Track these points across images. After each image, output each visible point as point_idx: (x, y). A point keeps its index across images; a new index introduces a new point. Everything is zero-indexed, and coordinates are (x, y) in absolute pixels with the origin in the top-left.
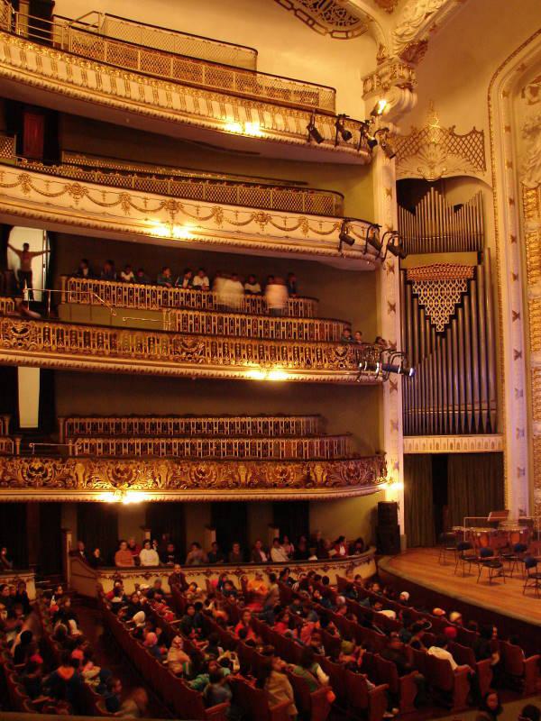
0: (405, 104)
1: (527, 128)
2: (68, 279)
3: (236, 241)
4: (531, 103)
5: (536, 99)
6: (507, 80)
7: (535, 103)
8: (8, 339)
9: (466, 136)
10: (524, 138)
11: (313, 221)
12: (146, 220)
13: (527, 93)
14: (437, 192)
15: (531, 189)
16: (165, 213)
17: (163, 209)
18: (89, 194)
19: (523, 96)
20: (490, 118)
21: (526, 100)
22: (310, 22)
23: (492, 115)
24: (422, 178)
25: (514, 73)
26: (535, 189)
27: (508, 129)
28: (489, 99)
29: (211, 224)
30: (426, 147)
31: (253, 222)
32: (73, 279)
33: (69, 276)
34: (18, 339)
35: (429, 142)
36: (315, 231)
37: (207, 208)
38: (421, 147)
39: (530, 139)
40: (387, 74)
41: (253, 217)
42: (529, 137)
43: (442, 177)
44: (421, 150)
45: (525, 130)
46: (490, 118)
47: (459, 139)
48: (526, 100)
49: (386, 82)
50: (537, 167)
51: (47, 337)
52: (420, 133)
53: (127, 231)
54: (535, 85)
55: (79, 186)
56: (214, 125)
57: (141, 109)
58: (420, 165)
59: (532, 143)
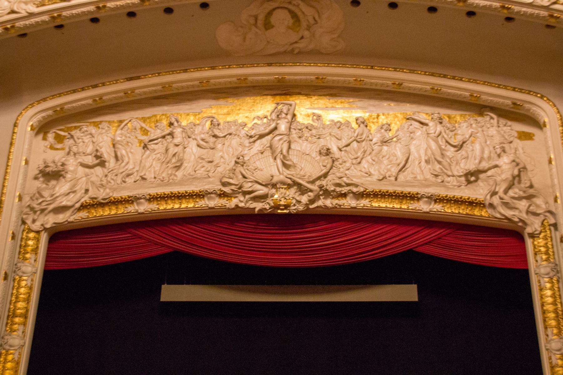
1: (48, 170)
4: (52, 148)
5: (59, 146)
6: (44, 114)
7: (57, 149)
10: (36, 178)
13: (51, 136)
15: (33, 231)
19: (44, 139)
20: (11, 144)
21: (47, 143)
23: (16, 142)
25: (50, 112)
26: (38, 232)
27: (27, 162)
28: (15, 125)
39: (43, 182)
42: (41, 179)
45: (41, 171)
46: (11, 144)
48: (47, 143)
50: (46, 212)
54: (62, 133)
59: (44, 186)
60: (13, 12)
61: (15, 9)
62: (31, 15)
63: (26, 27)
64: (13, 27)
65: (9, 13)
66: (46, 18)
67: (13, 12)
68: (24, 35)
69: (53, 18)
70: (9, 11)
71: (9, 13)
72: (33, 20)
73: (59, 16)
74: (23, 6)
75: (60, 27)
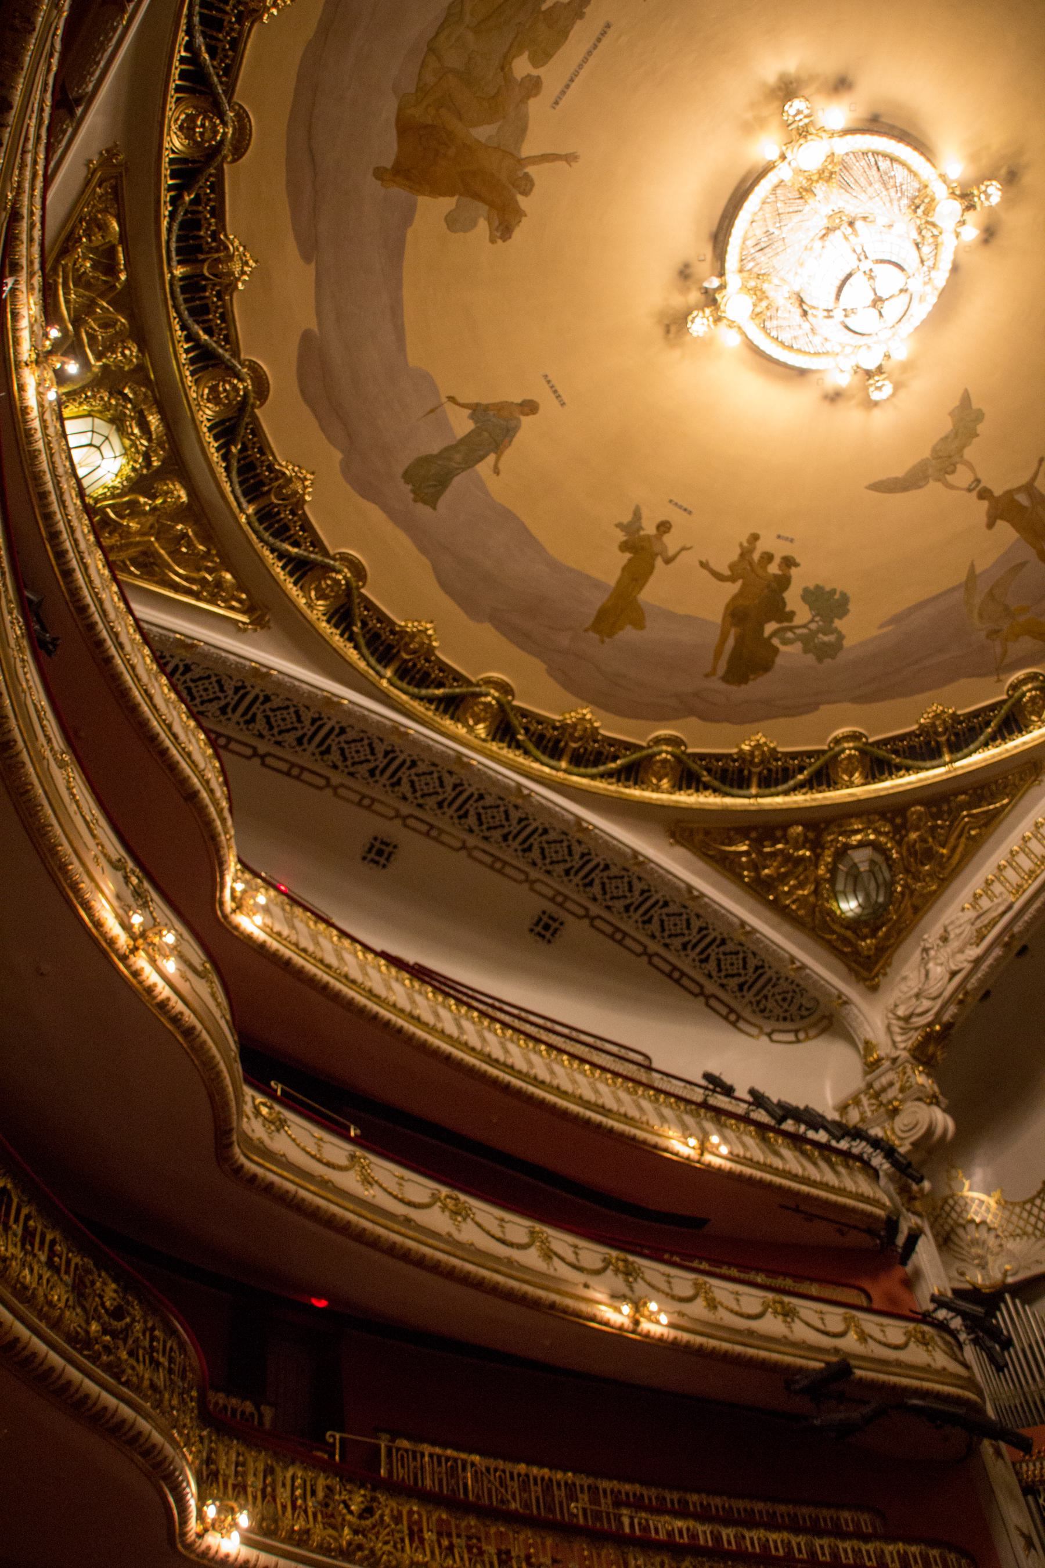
0: (939, 1131)
2: (393, 1441)
3: (751, 1351)
8: (334, 1528)
9: (1032, 1201)
11: (870, 1323)
12: (586, 1286)
14: (1017, 1301)
16: (615, 1281)
17: (609, 1272)
18: (478, 1219)
22: (733, 1017)
24: (968, 1286)
29: (698, 1308)
30: (960, 1231)
31: (769, 1315)
32: (405, 1444)
33: (395, 1435)
34: (356, 1532)
35: (961, 1221)
36: (875, 1340)
37: (683, 1281)
38: (952, 1230)
40: (891, 1084)
41: (766, 1306)
43: (1010, 1280)
44: (953, 1236)
47: (1018, 1210)
49: (895, 1098)
51: (415, 1534)
52: (946, 1202)
53: (553, 1306)
55: (457, 1199)
56: (652, 1139)
57: (531, 1089)
58: (958, 1264)
60: (953, 974)
61: (954, 968)
62: (977, 961)
63: (982, 981)
64: (966, 994)
65: (950, 979)
66: (997, 952)
67: (953, 974)
68: (987, 994)
69: (1007, 945)
70: (947, 977)
71: (950, 979)
72: (984, 967)
73: (1012, 936)
74: (960, 957)
75: (1023, 950)
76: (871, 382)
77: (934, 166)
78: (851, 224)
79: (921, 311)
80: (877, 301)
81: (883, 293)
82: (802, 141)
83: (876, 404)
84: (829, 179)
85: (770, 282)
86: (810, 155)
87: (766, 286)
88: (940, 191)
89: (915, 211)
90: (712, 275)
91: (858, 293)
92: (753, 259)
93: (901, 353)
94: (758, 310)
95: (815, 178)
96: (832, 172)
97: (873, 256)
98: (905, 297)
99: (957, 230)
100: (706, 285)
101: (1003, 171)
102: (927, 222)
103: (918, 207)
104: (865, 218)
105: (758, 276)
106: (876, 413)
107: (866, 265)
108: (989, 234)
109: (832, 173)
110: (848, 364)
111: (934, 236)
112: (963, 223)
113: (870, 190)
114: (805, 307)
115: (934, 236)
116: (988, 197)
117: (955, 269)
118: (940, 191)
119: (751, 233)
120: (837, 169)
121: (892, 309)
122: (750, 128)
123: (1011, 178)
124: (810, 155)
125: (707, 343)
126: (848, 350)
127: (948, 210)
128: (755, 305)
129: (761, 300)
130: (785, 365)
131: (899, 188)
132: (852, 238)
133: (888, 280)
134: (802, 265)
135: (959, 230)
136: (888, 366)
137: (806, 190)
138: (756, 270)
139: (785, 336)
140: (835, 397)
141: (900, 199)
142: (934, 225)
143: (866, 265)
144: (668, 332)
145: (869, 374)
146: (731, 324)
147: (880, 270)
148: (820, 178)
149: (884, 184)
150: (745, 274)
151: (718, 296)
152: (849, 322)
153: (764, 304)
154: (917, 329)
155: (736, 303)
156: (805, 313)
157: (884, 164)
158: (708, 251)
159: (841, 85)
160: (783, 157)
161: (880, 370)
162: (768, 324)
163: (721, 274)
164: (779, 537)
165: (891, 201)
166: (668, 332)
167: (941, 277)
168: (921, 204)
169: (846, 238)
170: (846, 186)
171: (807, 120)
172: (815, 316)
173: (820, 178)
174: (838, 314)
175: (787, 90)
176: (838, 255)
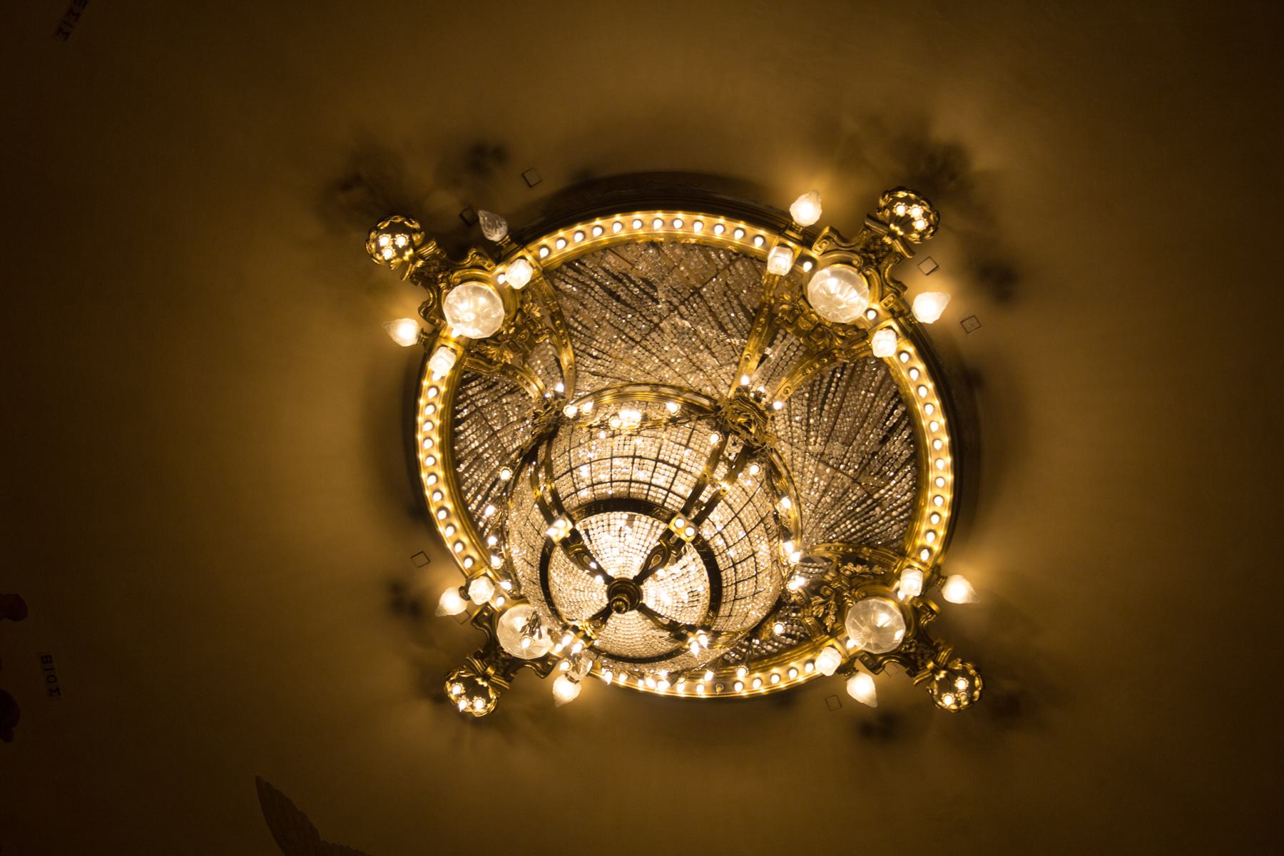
76: (477, 664)
77: (948, 542)
78: (749, 453)
79: (657, 683)
80: (625, 594)
81: (652, 593)
82: (856, 260)
83: (442, 699)
84: (812, 354)
85: (559, 347)
86: (841, 295)
87: (544, 339)
88: (910, 584)
89: (845, 559)
90: (509, 219)
91: (621, 544)
92: (585, 288)
93: (565, 690)
94: (492, 351)
95: (804, 325)
96: (832, 356)
97: (706, 532)
98: (662, 641)
99: (848, 662)
100: (483, 217)
101: (1008, 686)
102: (838, 594)
103: (858, 561)
104: (772, 472)
105: (557, 315)
106: (423, 711)
107: (682, 528)
108: (881, 726)
109: (828, 353)
110: (481, 591)
111: (820, 620)
112: (873, 663)
113: (836, 449)
114: (542, 452)
115: (820, 620)
116: (948, 686)
117: (784, 699)
118: (910, 584)
119: (629, 256)
120: (842, 359)
121: (628, 629)
122: (831, 146)
123: (1002, 707)
124: (841, 295)
125: (373, 285)
126: (506, 585)
127: (884, 621)
128: (496, 339)
129: (514, 348)
130: (414, 467)
131: (870, 501)
132: (722, 469)
133: (678, 589)
134: (622, 397)
135: (858, 664)
136: (526, 678)
137: (772, 316)
138: (568, 304)
139: (471, 437)
140: (412, 607)
141: (850, 515)
142: (841, 613)
143: (682, 528)
144: (346, 186)
145: (490, 649)
146: (433, 317)
147: (691, 558)
148: (807, 335)
149: (864, 468)
150: (546, 286)
151: (472, 257)
152: (559, 555)
153: (509, 357)
154: (630, 692)
155: (471, 312)
156: (528, 455)
157: (897, 446)
158: (550, 184)
159: (993, 277)
160: (808, 237)
161: (511, 666)
162: (474, 389)
163: (523, 237)
164: (46, 659)
165: (837, 501)
166: (346, 186)
167: (747, 683)
168: (863, 561)
169: (716, 457)
170: (815, 395)
171: (899, 248)
172: (534, 481)
173: (807, 335)
174: (560, 529)
175: (936, 176)
176: (681, 461)
